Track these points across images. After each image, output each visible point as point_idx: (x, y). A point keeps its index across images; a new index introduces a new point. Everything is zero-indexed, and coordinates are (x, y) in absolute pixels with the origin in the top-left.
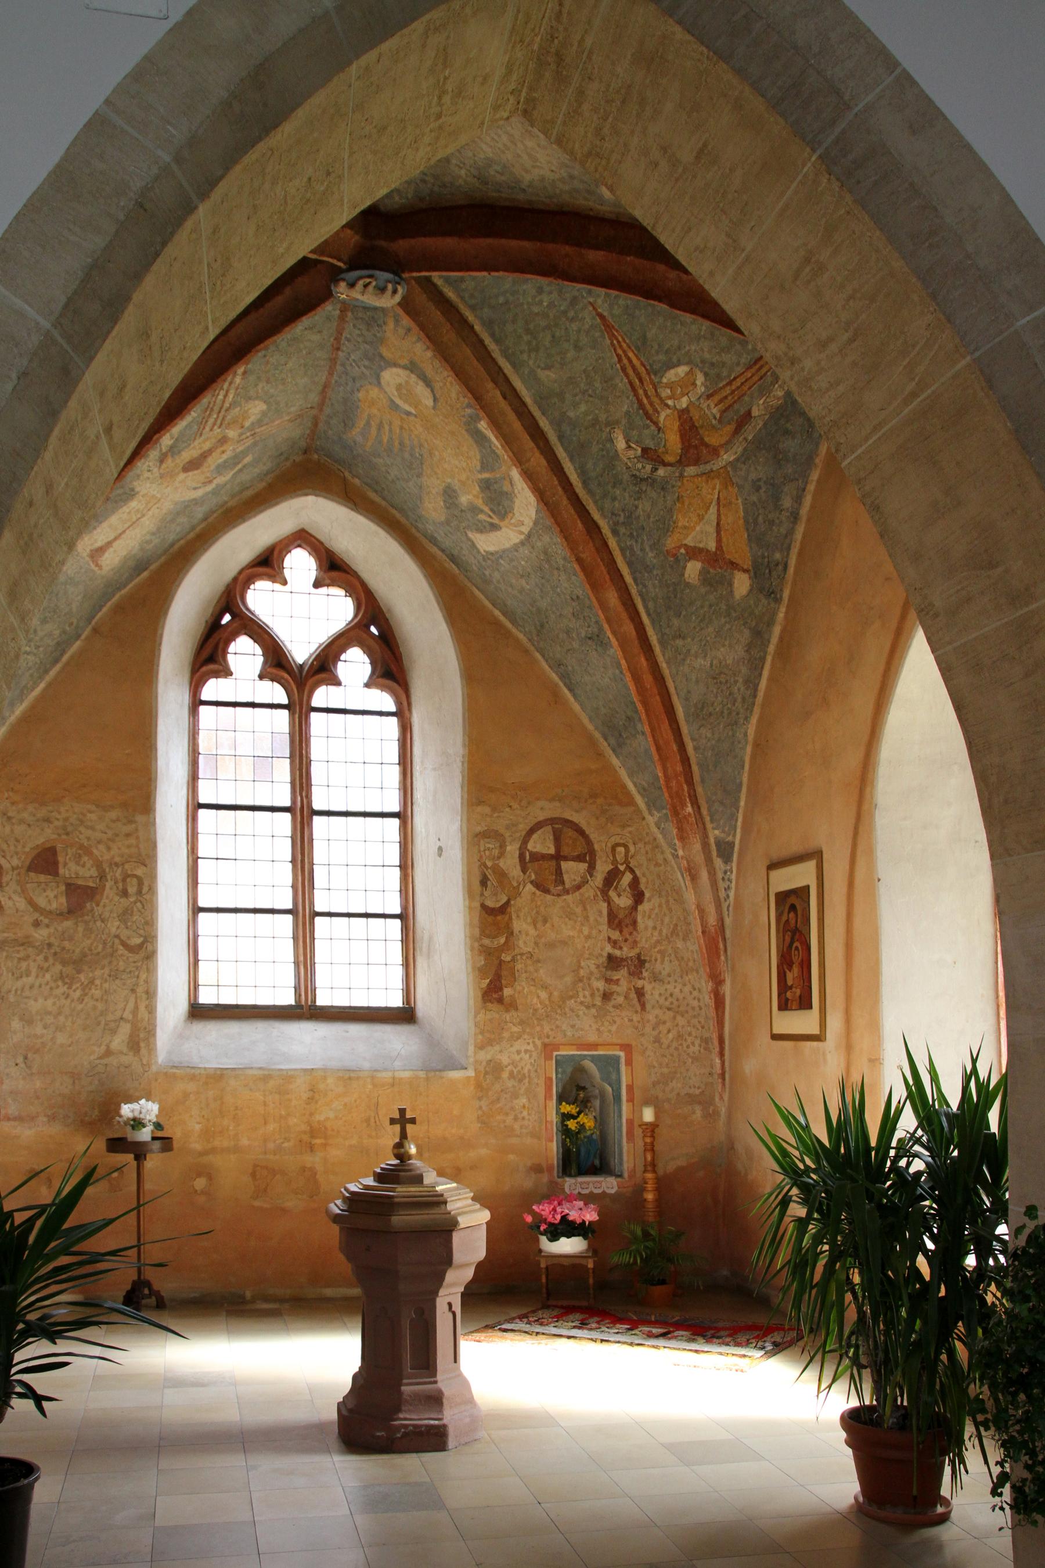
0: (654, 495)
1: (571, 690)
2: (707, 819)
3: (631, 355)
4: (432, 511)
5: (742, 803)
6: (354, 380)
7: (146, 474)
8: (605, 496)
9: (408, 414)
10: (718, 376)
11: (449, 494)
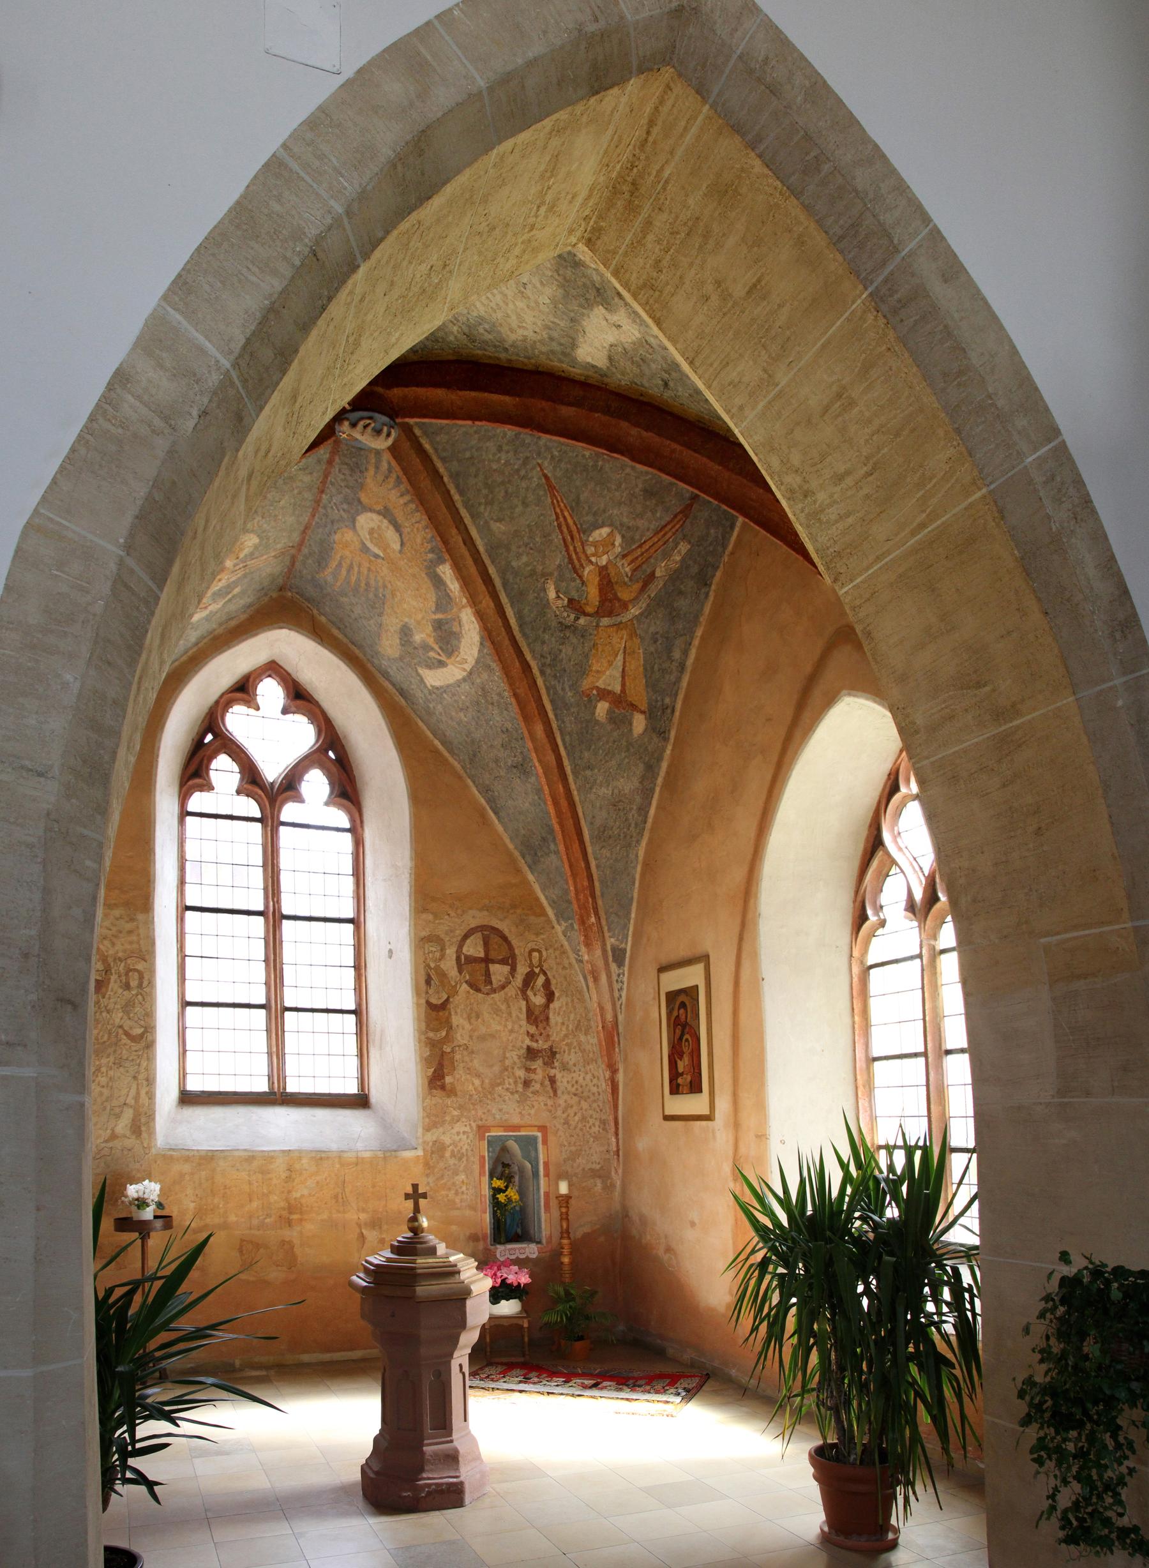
0: (575, 641)
1: (496, 813)
2: (606, 928)
3: (566, 514)
4: (389, 647)
5: (633, 915)
6: (332, 522)
8: (535, 641)
9: (377, 556)
10: (632, 538)
11: (405, 633)
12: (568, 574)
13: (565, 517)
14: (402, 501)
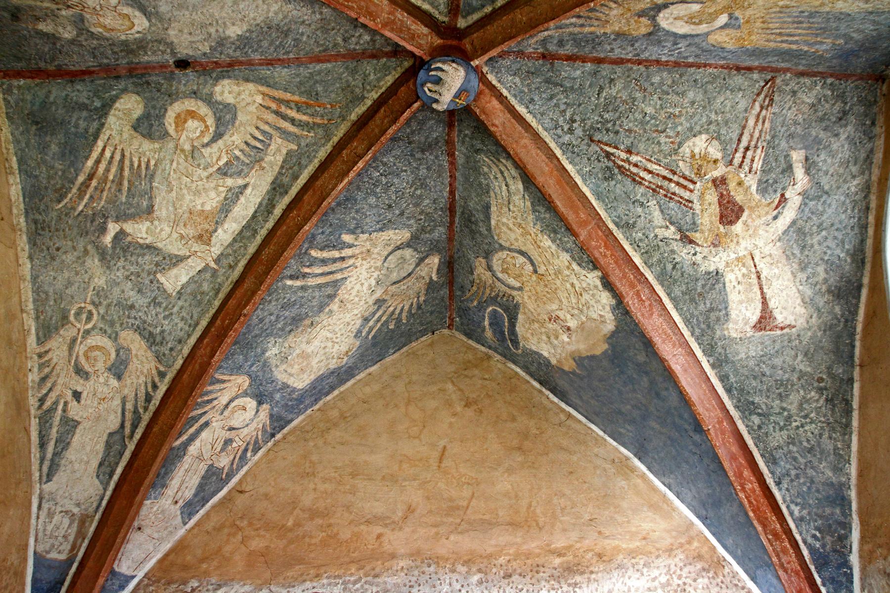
7: (699, 257)
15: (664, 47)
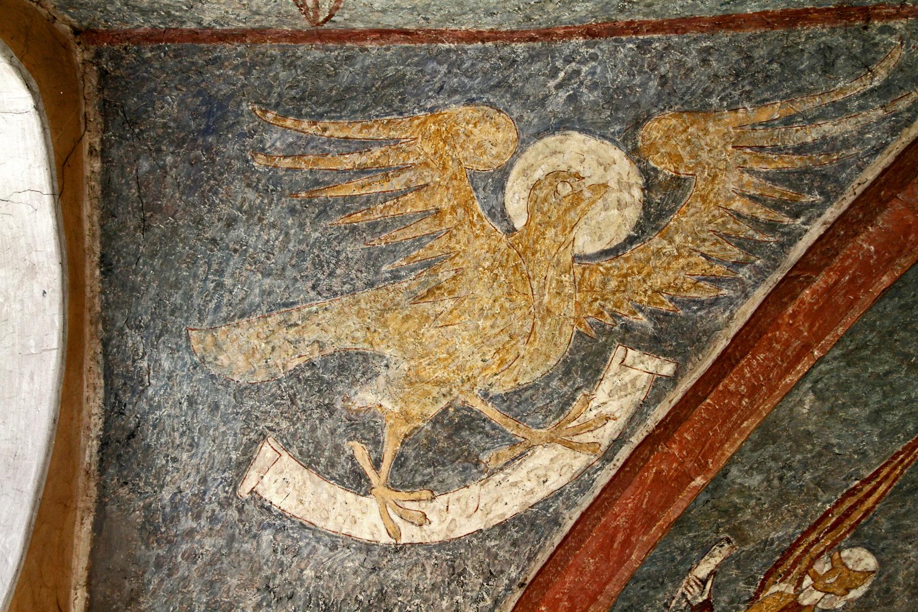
3: (883, 488)
12: (758, 569)
13: (875, 489)
14: (737, 205)
15: (594, 86)
